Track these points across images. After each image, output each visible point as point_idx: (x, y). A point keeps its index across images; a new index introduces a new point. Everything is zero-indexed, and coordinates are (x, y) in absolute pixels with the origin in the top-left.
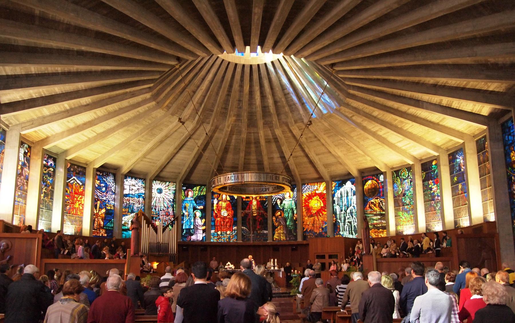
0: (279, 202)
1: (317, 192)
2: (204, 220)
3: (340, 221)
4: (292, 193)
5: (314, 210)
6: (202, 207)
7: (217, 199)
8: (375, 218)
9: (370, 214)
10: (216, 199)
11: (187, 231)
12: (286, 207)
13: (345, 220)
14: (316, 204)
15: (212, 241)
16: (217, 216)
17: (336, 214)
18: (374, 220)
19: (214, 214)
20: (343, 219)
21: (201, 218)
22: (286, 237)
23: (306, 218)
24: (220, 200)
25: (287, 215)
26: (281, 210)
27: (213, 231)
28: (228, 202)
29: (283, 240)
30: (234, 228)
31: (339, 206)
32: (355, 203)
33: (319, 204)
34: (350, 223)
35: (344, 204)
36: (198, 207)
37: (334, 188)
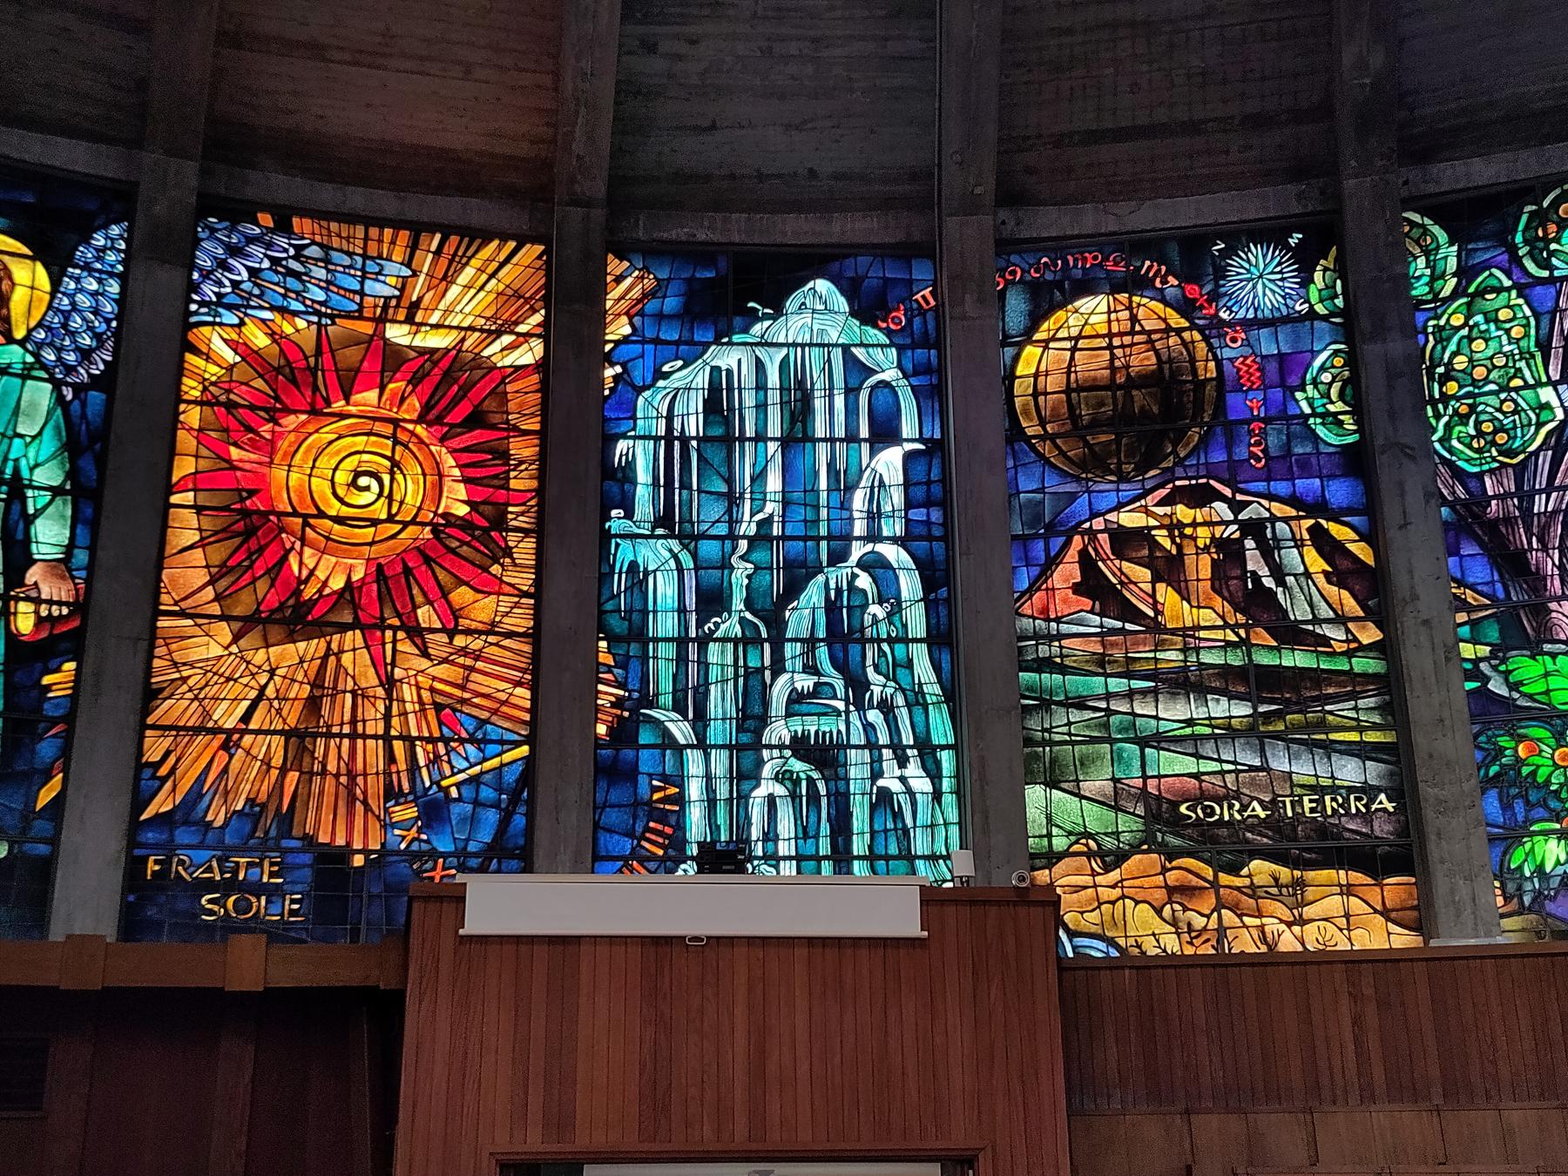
1: (397, 334)
3: (681, 731)
5: (329, 546)
8: (1173, 712)
9: (1101, 664)
13: (752, 718)
14: (352, 478)
17: (638, 634)
18: (1160, 740)
20: (721, 702)
31: (690, 539)
32: (893, 527)
33: (411, 490)
34: (823, 755)
35: (748, 528)
37: (620, 328)
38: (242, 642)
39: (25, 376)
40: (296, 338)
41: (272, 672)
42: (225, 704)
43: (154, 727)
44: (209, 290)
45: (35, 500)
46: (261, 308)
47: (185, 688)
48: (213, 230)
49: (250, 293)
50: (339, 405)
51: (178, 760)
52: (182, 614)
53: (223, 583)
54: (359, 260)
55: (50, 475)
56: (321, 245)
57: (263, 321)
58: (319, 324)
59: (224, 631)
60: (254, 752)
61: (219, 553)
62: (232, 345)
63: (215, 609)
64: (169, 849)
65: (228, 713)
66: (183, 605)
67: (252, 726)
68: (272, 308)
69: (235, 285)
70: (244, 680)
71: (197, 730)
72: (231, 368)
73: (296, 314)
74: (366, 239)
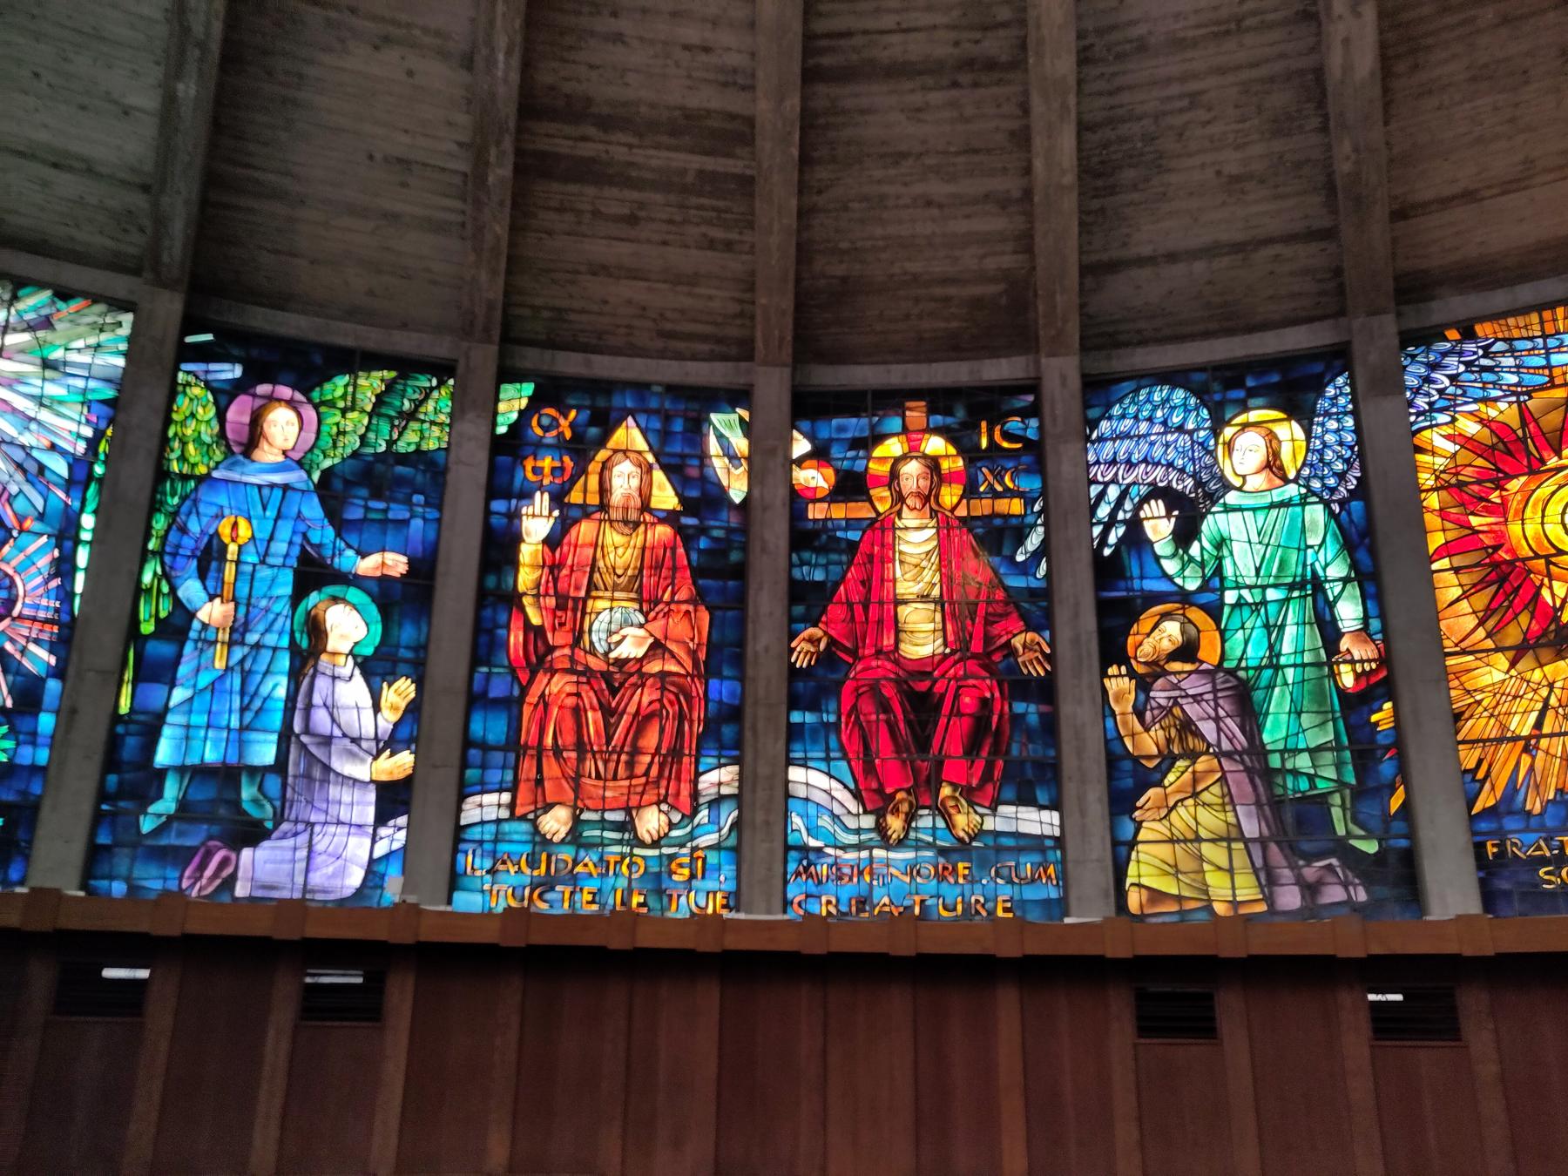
0: (1159, 527)
2: (400, 693)
4: (1290, 433)
6: (397, 564)
7: (558, 499)
10: (541, 501)
11: (204, 792)
12: (1242, 562)
15: (467, 901)
16: (539, 656)
19: (516, 638)
21: (376, 669)
22: (1268, 879)
23: (1493, 673)
24: (585, 511)
25: (1257, 653)
26: (1184, 597)
27: (484, 807)
28: (663, 531)
29: (1242, 921)
30: (708, 781)
36: (350, 561)
38: (1519, 666)
39: (1303, 502)
40: (1500, 418)
41: (1551, 686)
42: (1517, 718)
43: (1464, 742)
44: (1421, 402)
45: (1333, 590)
46: (1466, 403)
47: (1480, 709)
48: (1413, 357)
49: (1455, 395)
50: (1553, 462)
51: (1490, 766)
52: (1464, 652)
53: (1491, 623)
54: (1540, 341)
55: (1338, 569)
56: (1504, 340)
57: (1471, 413)
58: (1518, 402)
59: (1502, 661)
60: (1552, 751)
61: (1482, 599)
62: (1448, 437)
63: (1489, 644)
64: (1501, 835)
65: (1522, 723)
66: (1463, 645)
67: (1546, 730)
68: (1476, 401)
69: (1441, 392)
70: (1530, 695)
71: (1500, 740)
72: (1454, 455)
73: (1496, 400)
74: (1542, 322)
